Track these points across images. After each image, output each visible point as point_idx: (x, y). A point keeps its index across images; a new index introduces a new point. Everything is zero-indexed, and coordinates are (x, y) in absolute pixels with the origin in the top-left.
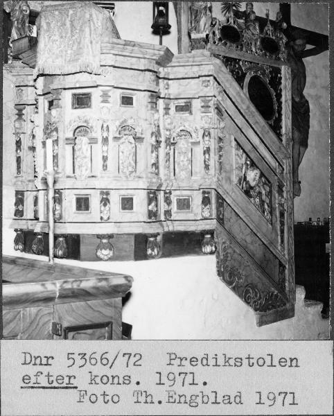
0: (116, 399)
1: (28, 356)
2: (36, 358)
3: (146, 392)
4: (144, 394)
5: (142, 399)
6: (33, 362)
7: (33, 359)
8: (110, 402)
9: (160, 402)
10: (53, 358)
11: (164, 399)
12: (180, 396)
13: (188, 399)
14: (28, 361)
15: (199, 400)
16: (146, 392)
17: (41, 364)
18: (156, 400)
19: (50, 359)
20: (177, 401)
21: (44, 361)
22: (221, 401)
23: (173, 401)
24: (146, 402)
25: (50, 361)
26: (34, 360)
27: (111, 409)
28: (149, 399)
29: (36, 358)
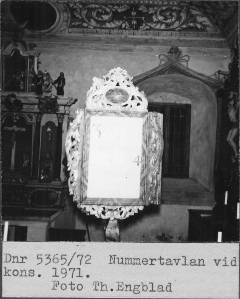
0: (80, 287)
1: (8, 256)
2: (14, 258)
3: (102, 283)
4: (100, 284)
5: (99, 288)
7: (12, 258)
10: (26, 258)
11: (115, 287)
12: (127, 286)
13: (132, 288)
14: (8, 260)
15: (140, 288)
16: (102, 283)
17: (17, 262)
18: (109, 289)
19: (24, 259)
21: (20, 260)
22: (156, 290)
23: (122, 289)
27: (76, 294)
28: (104, 288)
29: (14, 258)
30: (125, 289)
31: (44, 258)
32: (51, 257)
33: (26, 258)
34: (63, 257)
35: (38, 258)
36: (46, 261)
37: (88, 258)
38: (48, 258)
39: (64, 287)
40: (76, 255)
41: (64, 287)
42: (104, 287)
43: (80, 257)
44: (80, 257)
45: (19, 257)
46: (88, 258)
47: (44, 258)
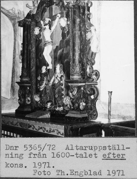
0: (49, 173)
1: (8, 146)
2: (11, 147)
4: (61, 171)
5: (60, 173)
9: (67, 174)
11: (69, 173)
15: (83, 174)
18: (66, 174)
19: (17, 147)
21: (15, 148)
23: (73, 174)
24: (61, 175)
26: (11, 148)
29: (11, 147)
30: (74, 174)
31: (28, 147)
33: (18, 147)
34: (39, 146)
36: (29, 149)
37: (54, 146)
38: (30, 147)
39: (40, 173)
40: (47, 145)
41: (40, 173)
44: (49, 146)
45: (14, 147)
46: (54, 146)
47: (28, 147)
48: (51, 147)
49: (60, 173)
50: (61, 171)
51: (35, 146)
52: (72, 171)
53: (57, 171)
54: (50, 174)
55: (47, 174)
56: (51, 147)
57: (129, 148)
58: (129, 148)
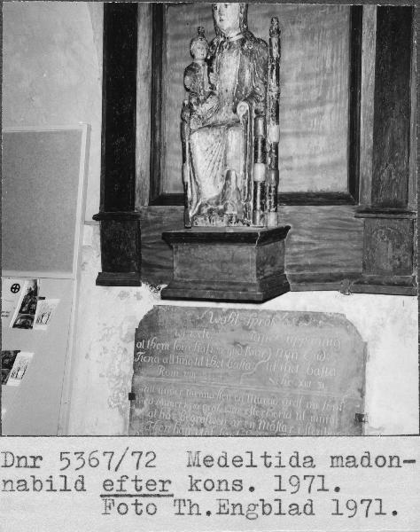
0: (151, 509)
4: (187, 503)
5: (185, 510)
6: (16, 464)
7: (16, 460)
8: (144, 512)
9: (209, 513)
10: (41, 458)
11: (214, 510)
18: (203, 511)
19: (38, 460)
20: (231, 511)
21: (30, 462)
23: (226, 511)
25: (38, 462)
29: (19, 458)
30: (231, 511)
32: (86, 457)
33: (41, 458)
35: (61, 459)
36: (76, 463)
37: (151, 456)
42: (195, 508)
43: (137, 455)
44: (137, 455)
46: (151, 456)
48: (144, 460)
49: (185, 510)
50: (187, 503)
51: (95, 455)
52: (222, 504)
53: (177, 503)
54: (155, 512)
55: (144, 510)
56: (144, 460)
57: (413, 461)
58: (413, 461)
